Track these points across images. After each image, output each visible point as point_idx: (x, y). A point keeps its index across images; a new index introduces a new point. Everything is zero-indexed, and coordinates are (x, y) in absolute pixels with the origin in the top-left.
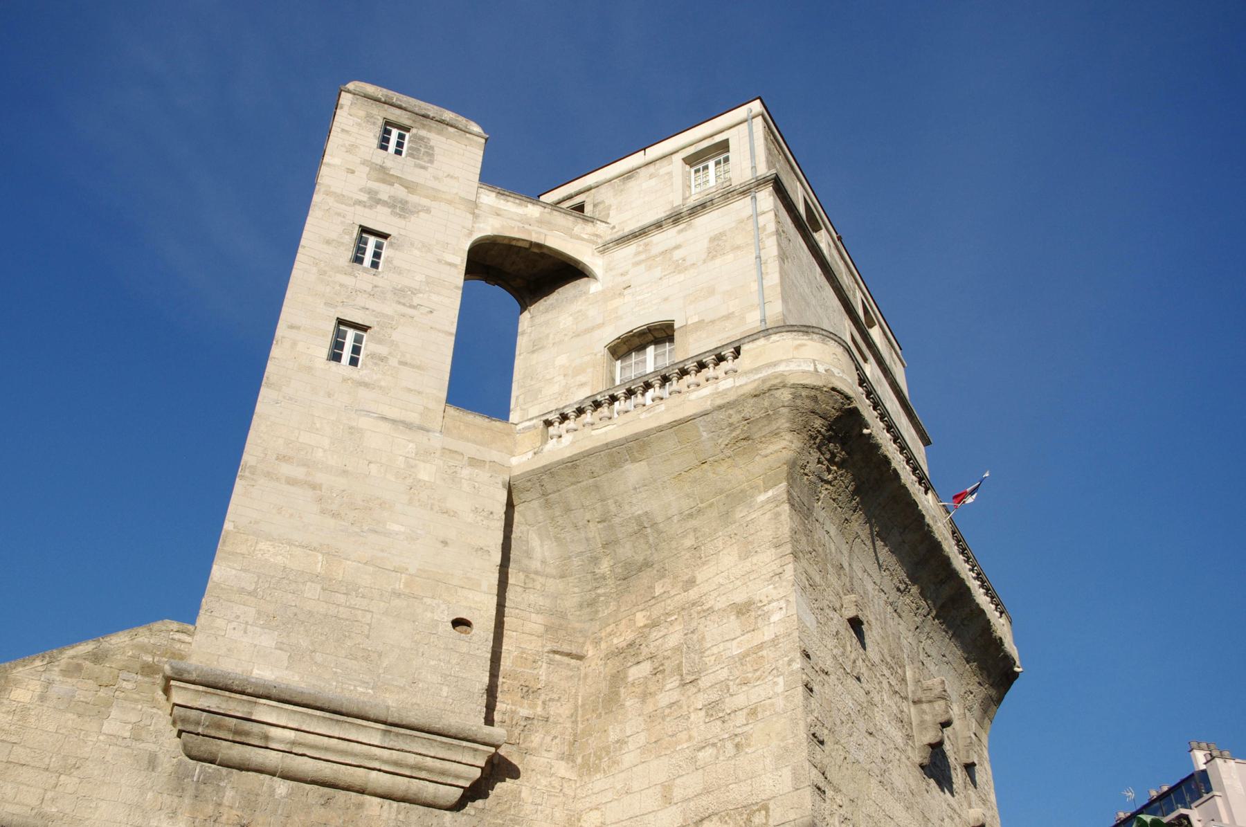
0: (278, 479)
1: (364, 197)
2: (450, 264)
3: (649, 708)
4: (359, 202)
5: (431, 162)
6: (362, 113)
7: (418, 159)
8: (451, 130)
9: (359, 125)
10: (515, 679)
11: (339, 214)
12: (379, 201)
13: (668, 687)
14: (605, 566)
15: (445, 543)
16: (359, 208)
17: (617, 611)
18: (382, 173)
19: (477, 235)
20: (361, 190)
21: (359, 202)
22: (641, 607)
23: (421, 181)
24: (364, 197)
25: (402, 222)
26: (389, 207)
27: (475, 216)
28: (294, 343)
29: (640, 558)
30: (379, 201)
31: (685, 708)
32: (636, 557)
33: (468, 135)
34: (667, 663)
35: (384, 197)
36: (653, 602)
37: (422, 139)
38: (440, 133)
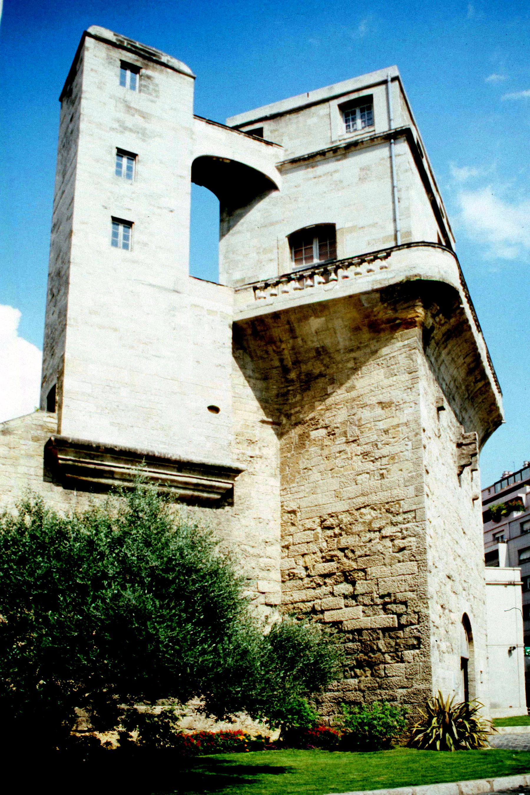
3: (326, 452)
4: (113, 129)
10: (243, 436)
12: (125, 128)
13: (337, 443)
14: (293, 375)
17: (302, 399)
21: (113, 129)
22: (318, 399)
29: (317, 371)
30: (125, 128)
31: (349, 454)
32: (314, 371)
34: (336, 430)
35: (129, 124)
36: (326, 397)
37: (149, 77)
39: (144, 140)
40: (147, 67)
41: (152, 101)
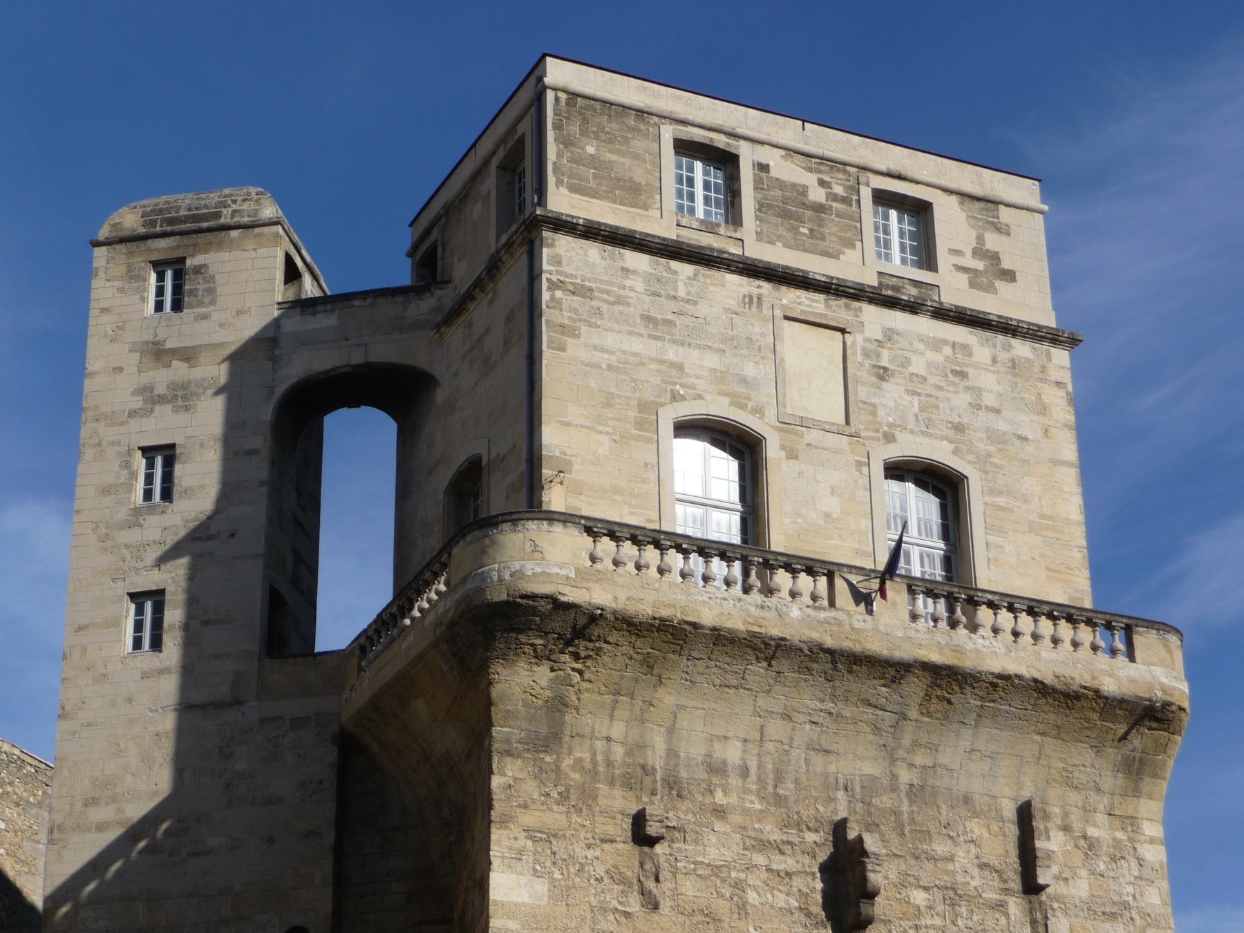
0: (89, 830)
1: (138, 402)
2: (252, 452)
4: (133, 414)
5: (213, 302)
6: (122, 269)
7: (198, 306)
8: (234, 234)
9: (121, 290)
11: (113, 444)
15: (271, 840)
16: (135, 424)
18: (158, 353)
19: (280, 390)
20: (133, 394)
21: (133, 414)
23: (205, 340)
24: (138, 402)
25: (183, 418)
26: (169, 402)
27: (274, 359)
28: (84, 650)
33: (257, 230)
35: (161, 390)
37: (198, 270)
38: (220, 246)
39: (187, 409)
40: (197, 249)
41: (204, 317)
